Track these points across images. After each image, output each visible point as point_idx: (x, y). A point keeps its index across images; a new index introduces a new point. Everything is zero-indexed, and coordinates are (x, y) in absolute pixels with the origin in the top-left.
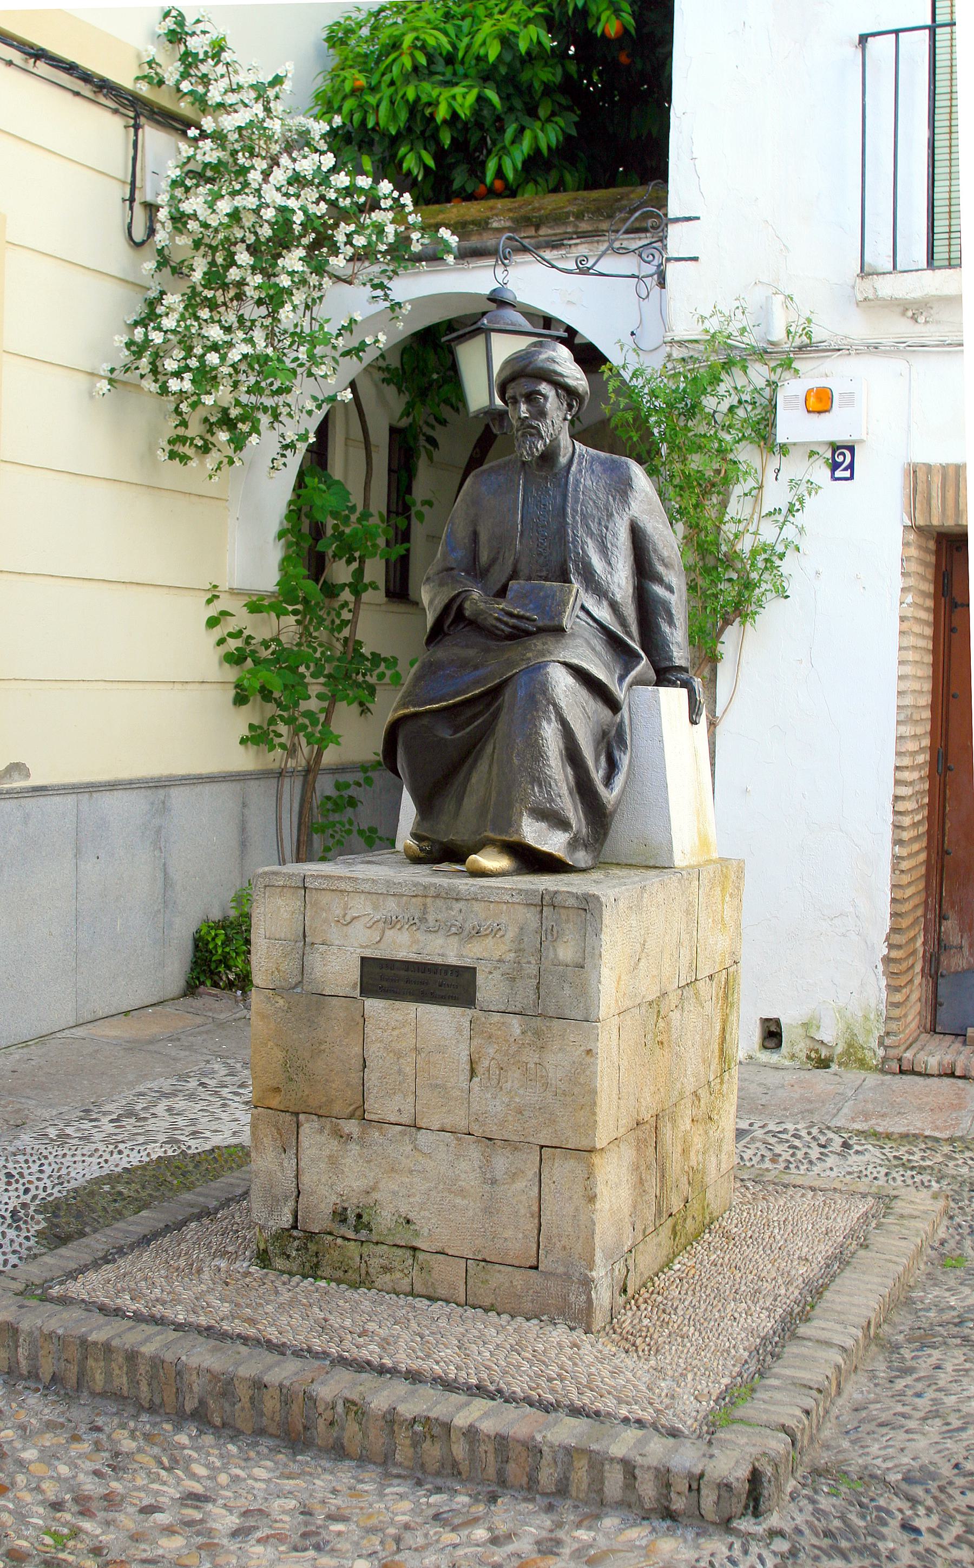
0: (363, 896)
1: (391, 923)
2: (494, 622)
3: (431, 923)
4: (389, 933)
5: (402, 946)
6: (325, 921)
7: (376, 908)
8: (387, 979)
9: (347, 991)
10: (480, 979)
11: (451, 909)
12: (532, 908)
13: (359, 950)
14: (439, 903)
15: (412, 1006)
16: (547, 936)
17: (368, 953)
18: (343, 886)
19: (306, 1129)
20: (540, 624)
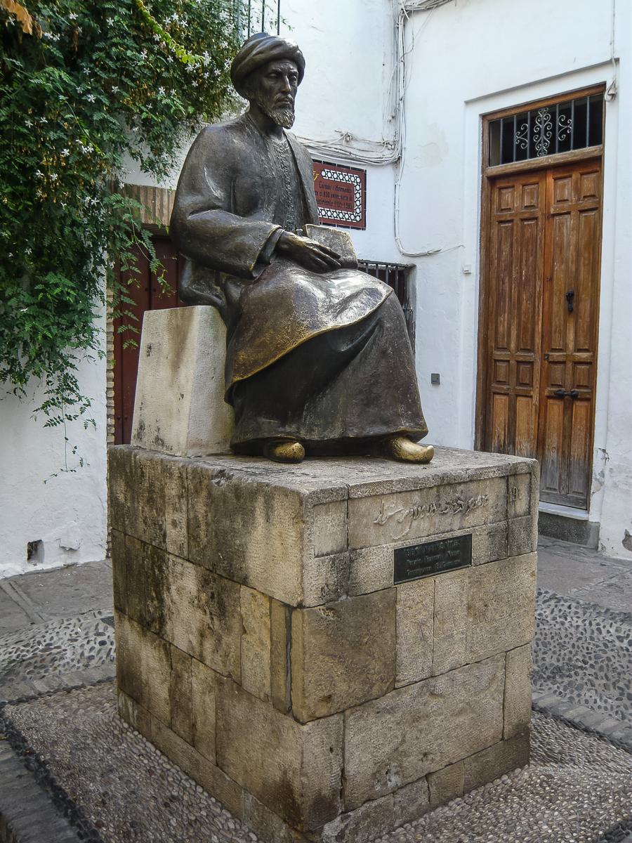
0: (395, 496)
1: (415, 514)
2: (313, 256)
3: (443, 506)
4: (415, 523)
5: (423, 531)
6: (366, 526)
7: (405, 504)
8: (415, 563)
9: (385, 583)
10: (475, 542)
11: (456, 492)
12: (502, 479)
13: (393, 544)
14: (448, 489)
15: (430, 580)
16: (510, 496)
17: (399, 545)
18: (380, 490)
19: (351, 721)
20: (342, 258)
